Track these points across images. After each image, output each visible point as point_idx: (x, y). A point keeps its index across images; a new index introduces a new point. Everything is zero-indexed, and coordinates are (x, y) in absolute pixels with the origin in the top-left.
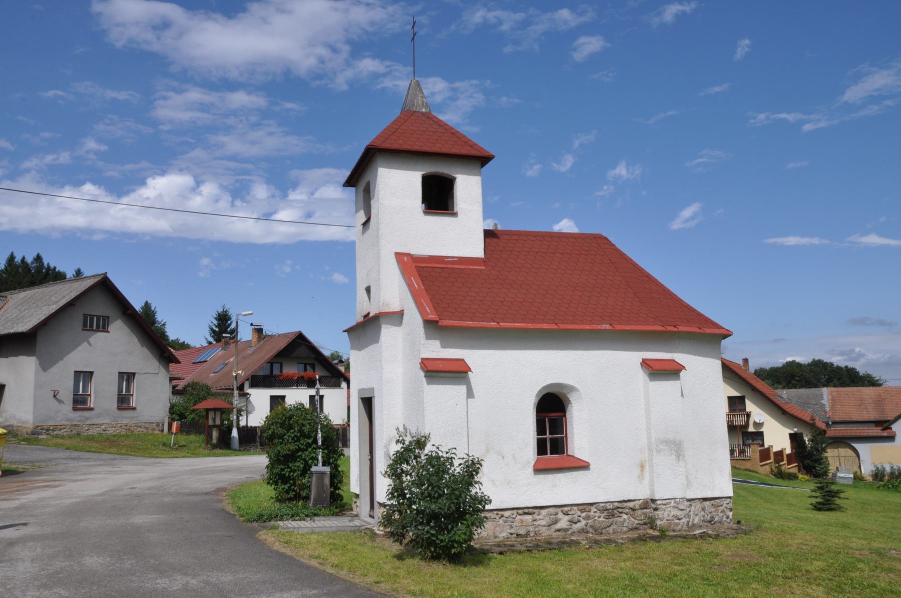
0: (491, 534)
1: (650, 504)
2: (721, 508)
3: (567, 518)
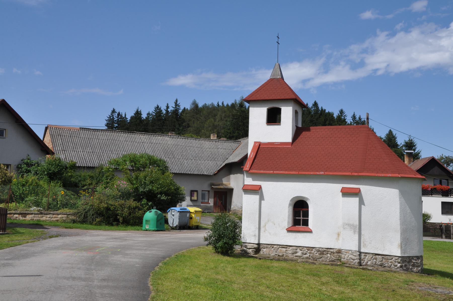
0: (268, 253)
1: (339, 251)
2: (390, 261)
3: (301, 252)
